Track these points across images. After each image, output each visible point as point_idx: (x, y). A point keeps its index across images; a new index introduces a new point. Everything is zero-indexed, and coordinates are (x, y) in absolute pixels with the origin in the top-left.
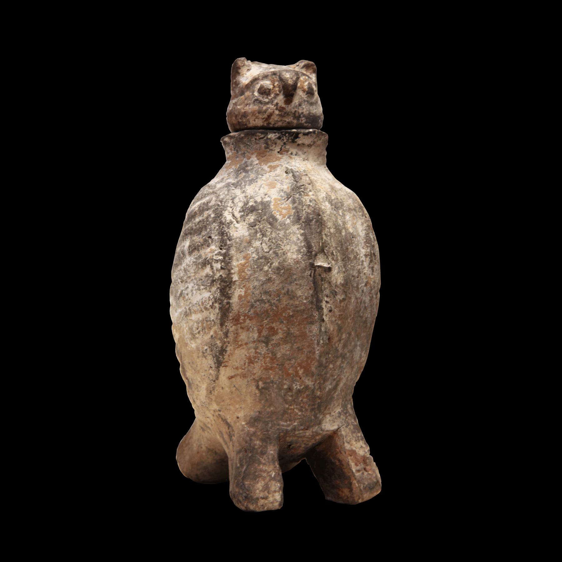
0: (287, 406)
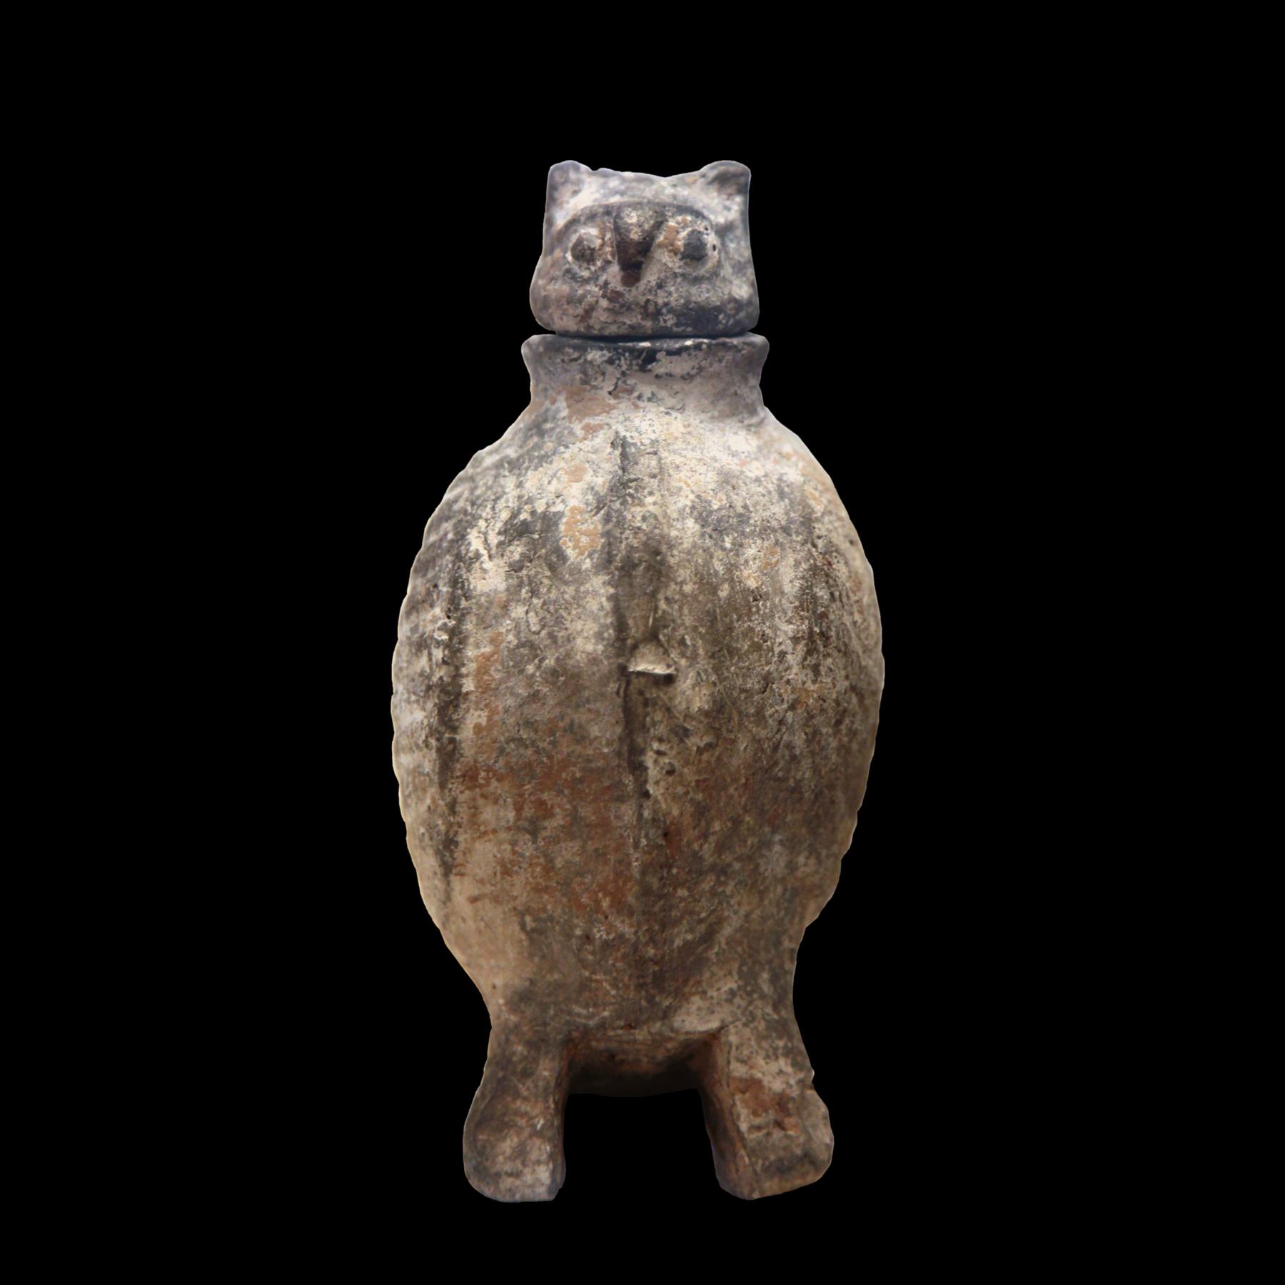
0: (587, 974)
